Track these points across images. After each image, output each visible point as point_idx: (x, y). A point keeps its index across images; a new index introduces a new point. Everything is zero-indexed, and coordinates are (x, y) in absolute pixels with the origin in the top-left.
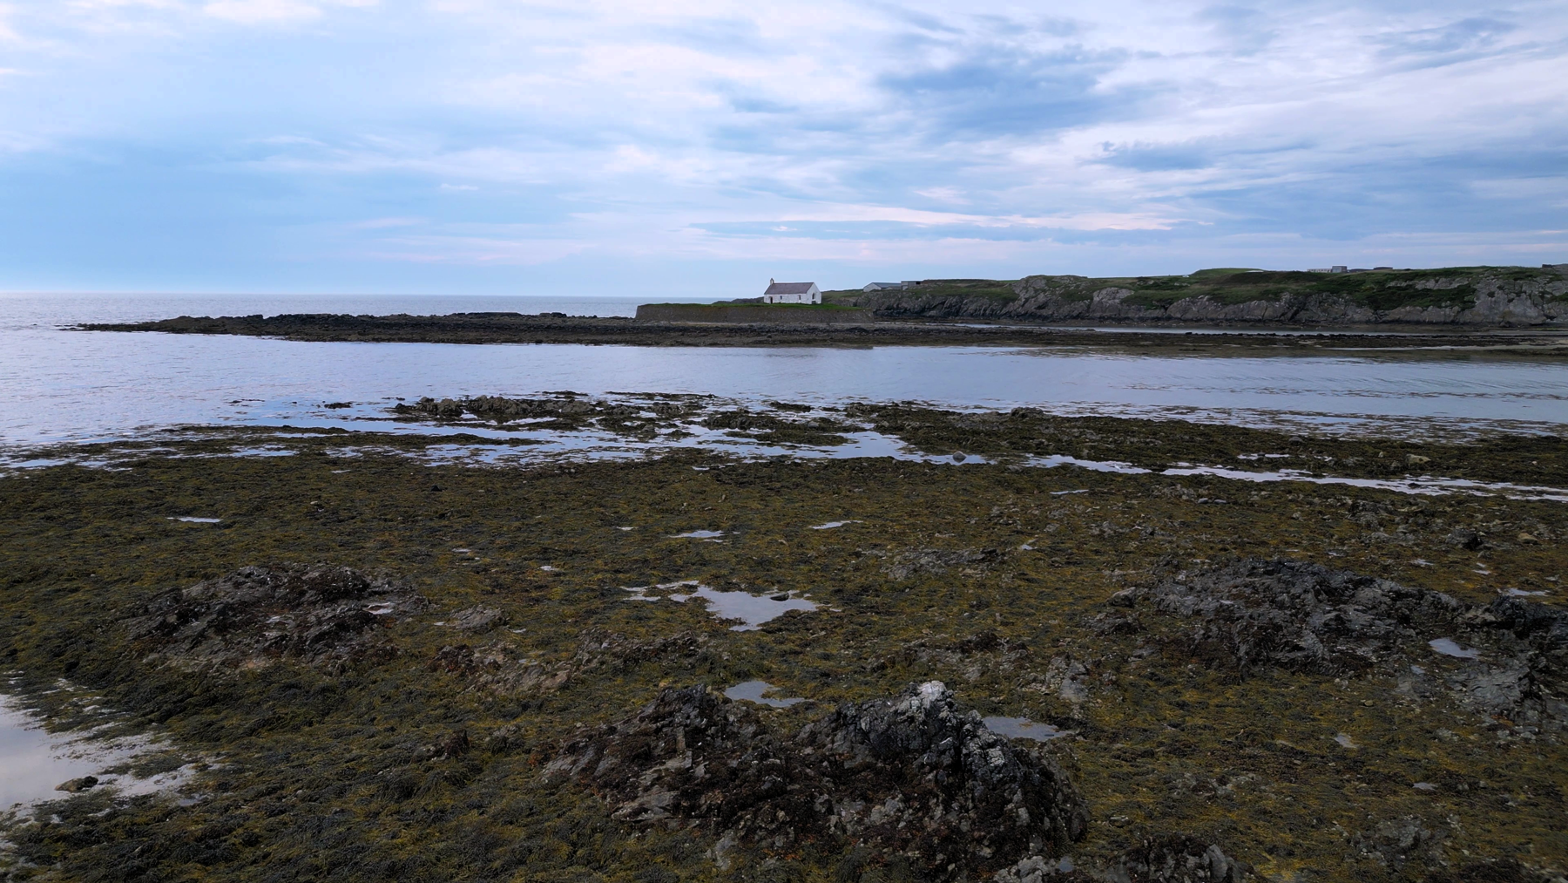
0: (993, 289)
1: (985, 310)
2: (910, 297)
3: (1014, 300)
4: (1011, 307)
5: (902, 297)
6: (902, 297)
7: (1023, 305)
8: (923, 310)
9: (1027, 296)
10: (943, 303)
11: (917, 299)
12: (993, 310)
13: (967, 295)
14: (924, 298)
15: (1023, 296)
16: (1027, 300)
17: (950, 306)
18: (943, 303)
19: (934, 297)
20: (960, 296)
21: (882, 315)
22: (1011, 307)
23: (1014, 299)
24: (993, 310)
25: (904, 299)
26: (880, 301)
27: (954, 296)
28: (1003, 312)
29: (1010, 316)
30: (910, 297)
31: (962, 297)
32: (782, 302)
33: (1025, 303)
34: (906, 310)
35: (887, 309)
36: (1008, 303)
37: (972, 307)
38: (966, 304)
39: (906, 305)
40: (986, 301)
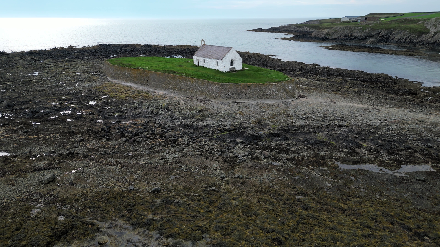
0: (412, 25)
1: (406, 39)
2: (359, 30)
3: (426, 33)
4: (424, 38)
5: (354, 30)
6: (354, 30)
7: (432, 37)
8: (366, 38)
9: (436, 31)
10: (379, 34)
11: (363, 31)
12: (411, 39)
13: (395, 29)
14: (367, 30)
15: (433, 31)
16: (436, 33)
17: (383, 36)
18: (379, 34)
19: (373, 30)
20: (390, 29)
21: (342, 40)
22: (424, 38)
23: (426, 32)
24: (411, 39)
25: (355, 31)
26: (341, 32)
27: (386, 29)
28: (418, 40)
29: (423, 44)
30: (359, 30)
31: (391, 30)
32: (205, 66)
33: (434, 35)
34: (355, 37)
35: (345, 36)
36: (422, 35)
37: (398, 37)
38: (394, 34)
39: (355, 34)
40: (407, 33)
